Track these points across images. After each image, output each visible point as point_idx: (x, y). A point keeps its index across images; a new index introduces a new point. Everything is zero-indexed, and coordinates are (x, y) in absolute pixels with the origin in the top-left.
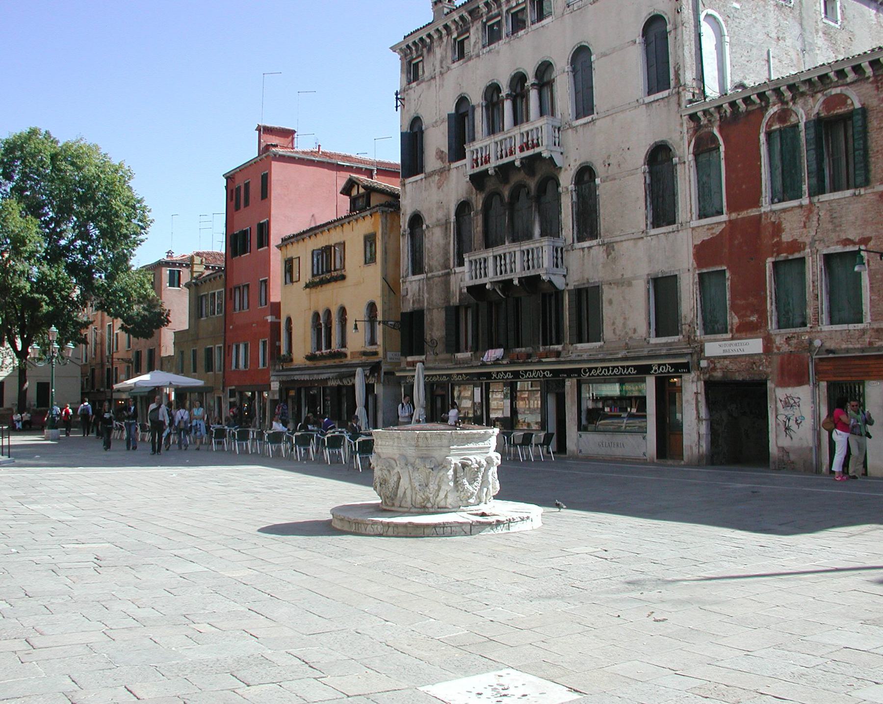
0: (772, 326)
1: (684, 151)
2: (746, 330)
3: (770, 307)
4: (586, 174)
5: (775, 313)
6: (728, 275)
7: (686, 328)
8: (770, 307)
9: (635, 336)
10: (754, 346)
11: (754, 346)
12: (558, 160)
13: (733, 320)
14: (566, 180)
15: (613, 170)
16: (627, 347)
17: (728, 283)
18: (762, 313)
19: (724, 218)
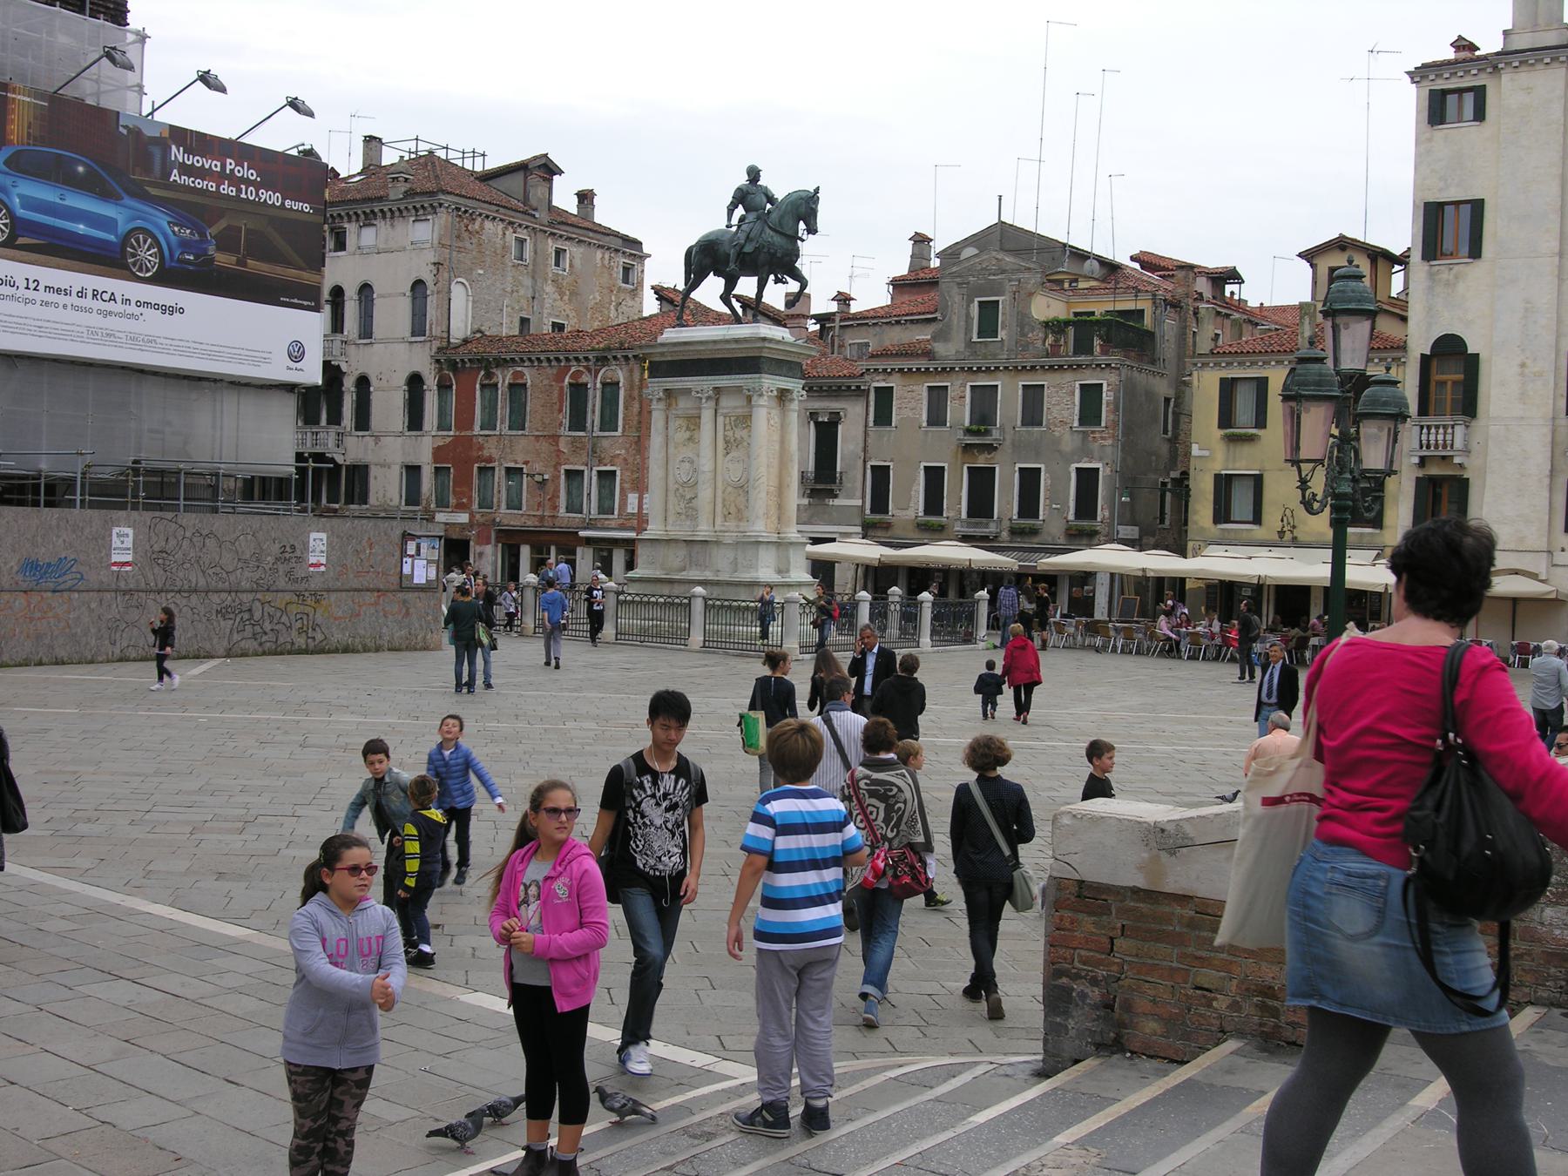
0: (475, 506)
1: (431, 382)
2: (461, 507)
3: (475, 495)
4: (363, 382)
5: (477, 499)
6: (452, 470)
7: (424, 502)
8: (475, 495)
9: (391, 504)
10: (463, 518)
11: (463, 518)
12: (344, 368)
13: (452, 501)
14: (349, 384)
15: (384, 383)
16: (385, 510)
17: (452, 476)
18: (470, 498)
19: (452, 433)
